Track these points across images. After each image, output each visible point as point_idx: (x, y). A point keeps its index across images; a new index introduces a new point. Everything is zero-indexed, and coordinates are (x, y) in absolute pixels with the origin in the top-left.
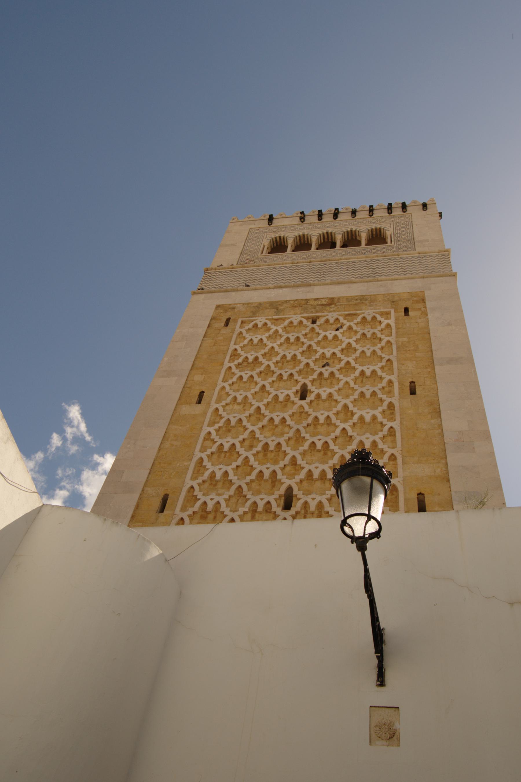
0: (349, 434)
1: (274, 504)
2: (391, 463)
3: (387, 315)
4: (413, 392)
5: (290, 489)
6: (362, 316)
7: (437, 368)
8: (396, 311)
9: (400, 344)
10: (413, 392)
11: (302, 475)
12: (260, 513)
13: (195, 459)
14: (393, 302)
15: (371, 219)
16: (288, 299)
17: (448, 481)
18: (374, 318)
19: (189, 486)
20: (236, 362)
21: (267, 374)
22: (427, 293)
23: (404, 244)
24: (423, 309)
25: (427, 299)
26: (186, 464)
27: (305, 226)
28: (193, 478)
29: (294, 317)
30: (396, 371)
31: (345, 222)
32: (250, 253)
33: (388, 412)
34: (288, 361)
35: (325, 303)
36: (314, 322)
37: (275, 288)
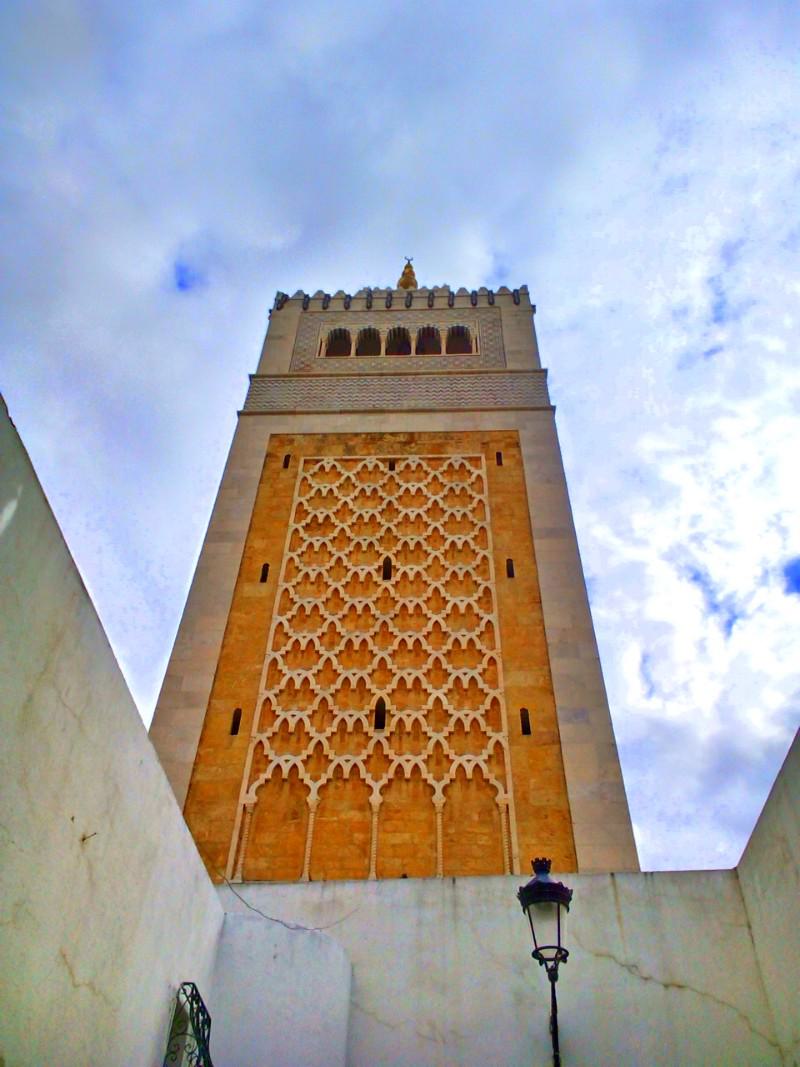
0: (443, 630)
1: (365, 721)
2: (491, 668)
3: (475, 461)
4: (511, 574)
5: (381, 703)
6: (448, 462)
7: (536, 542)
8: (487, 459)
9: (493, 505)
10: (511, 574)
11: (394, 684)
12: (350, 734)
13: (268, 661)
14: (484, 444)
15: (450, 312)
16: (359, 431)
17: (552, 693)
18: (462, 465)
19: (264, 698)
20: (303, 523)
21: (341, 541)
22: (522, 433)
23: (492, 355)
24: (517, 456)
26: (258, 667)
27: (371, 314)
28: (269, 687)
29: (368, 458)
30: (490, 544)
33: (484, 600)
34: (366, 524)
36: (392, 468)
37: (341, 412)
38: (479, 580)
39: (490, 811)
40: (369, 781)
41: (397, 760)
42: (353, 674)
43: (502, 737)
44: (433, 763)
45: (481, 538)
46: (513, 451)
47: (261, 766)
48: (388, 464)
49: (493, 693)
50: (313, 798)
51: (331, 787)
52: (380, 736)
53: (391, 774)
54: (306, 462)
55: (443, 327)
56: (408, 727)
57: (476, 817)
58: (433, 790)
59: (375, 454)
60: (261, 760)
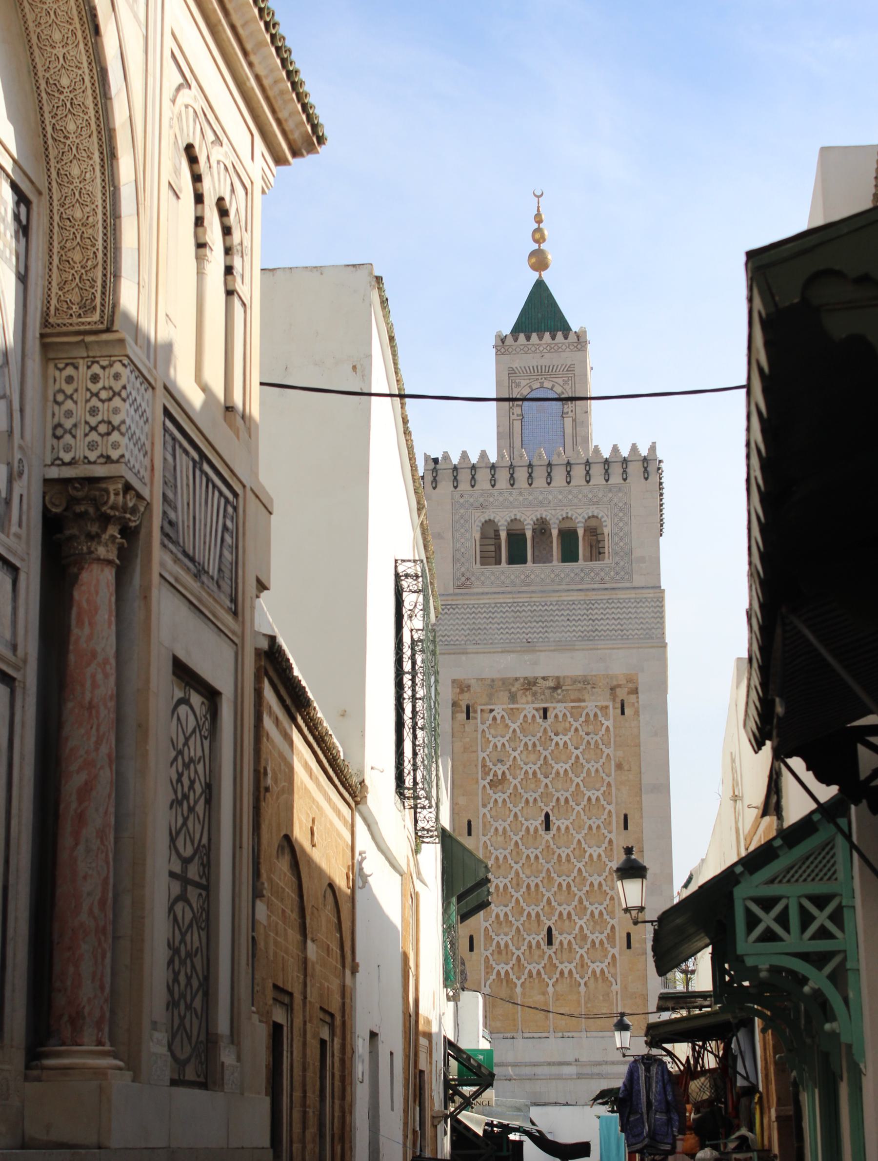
4: (626, 828)
5: (550, 930)
7: (643, 796)
8: (614, 708)
10: (626, 828)
16: (518, 675)
18: (596, 715)
24: (636, 704)
25: (640, 690)
27: (515, 492)
29: (527, 706)
31: (561, 492)
32: (463, 560)
33: (609, 848)
35: (552, 684)
37: (502, 652)
38: (605, 832)
39: (607, 995)
40: (547, 980)
41: (561, 966)
42: (533, 910)
43: (616, 951)
44: (579, 967)
45: (607, 794)
46: (633, 698)
47: (489, 970)
48: (542, 712)
49: (612, 922)
50: (519, 990)
51: (527, 982)
52: (550, 951)
53: (558, 975)
54: (482, 710)
55: (580, 519)
56: (565, 945)
57: (601, 998)
58: (580, 985)
59: (533, 702)
60: (489, 968)
